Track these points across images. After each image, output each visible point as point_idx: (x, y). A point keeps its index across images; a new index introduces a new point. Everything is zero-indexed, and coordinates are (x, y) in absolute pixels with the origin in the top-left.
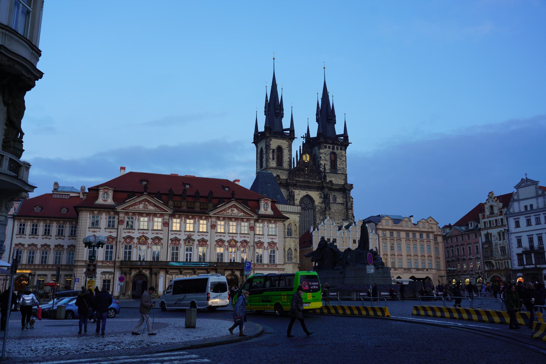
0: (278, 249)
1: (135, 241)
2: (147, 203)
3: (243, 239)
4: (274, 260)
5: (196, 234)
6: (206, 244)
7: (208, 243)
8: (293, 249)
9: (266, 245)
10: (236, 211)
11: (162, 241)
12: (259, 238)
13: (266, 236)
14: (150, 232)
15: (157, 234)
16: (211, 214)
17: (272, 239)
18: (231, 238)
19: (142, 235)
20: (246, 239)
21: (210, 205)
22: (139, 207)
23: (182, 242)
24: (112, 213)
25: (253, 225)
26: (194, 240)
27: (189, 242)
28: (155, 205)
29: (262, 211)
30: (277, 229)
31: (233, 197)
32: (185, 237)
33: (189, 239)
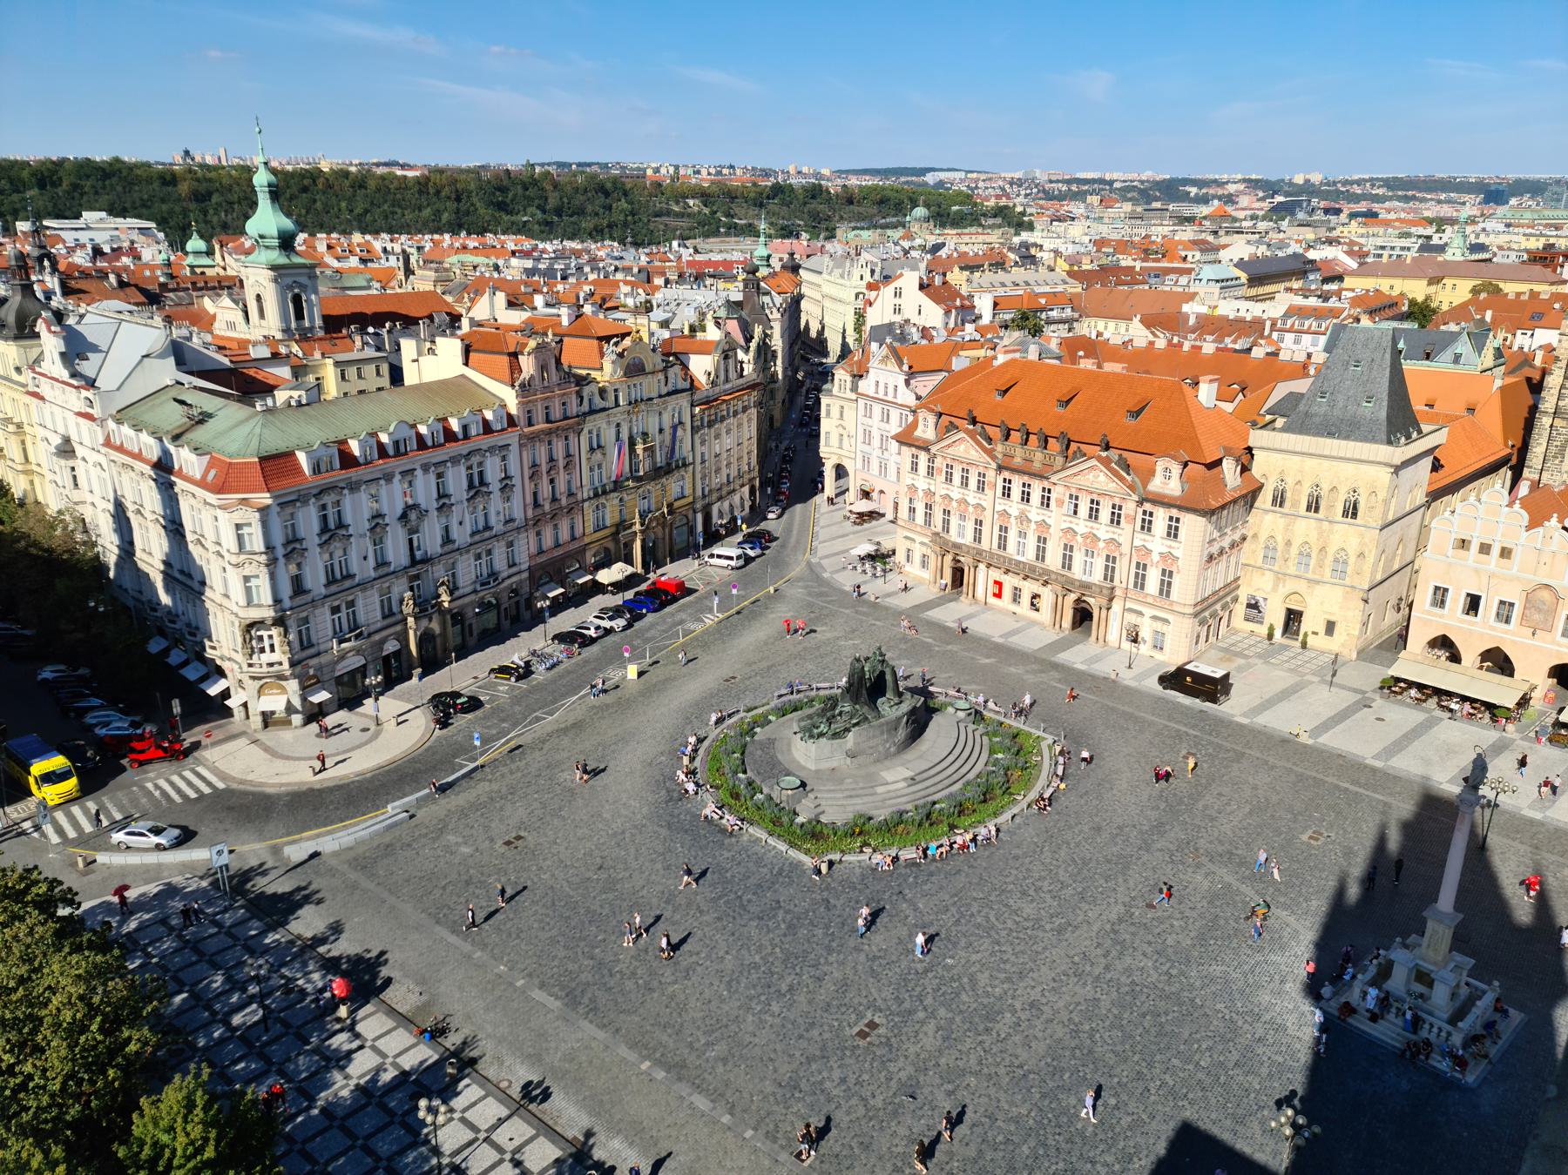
4: (1168, 593)
9: (1155, 557)
10: (1102, 478)
13: (1157, 540)
14: (972, 494)
16: (1054, 479)
23: (1012, 520)
29: (1157, 485)
33: (1023, 518)
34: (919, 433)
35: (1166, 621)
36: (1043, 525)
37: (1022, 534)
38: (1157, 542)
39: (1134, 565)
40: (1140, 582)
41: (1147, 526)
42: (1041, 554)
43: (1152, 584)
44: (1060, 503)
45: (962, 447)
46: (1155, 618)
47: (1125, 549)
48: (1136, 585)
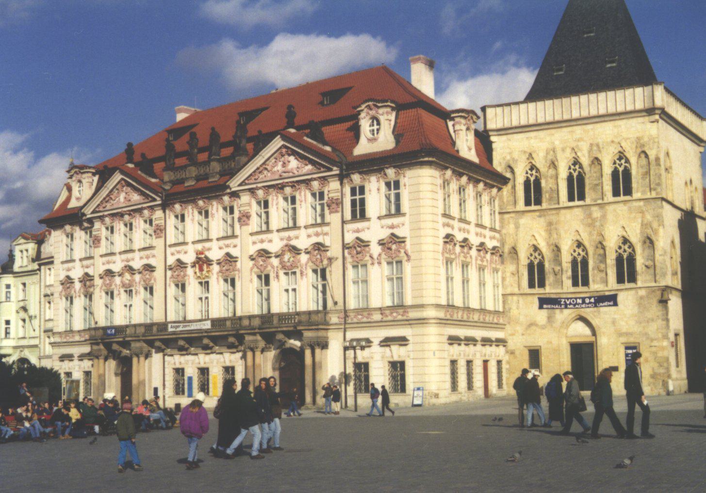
0: (409, 260)
2: (129, 189)
5: (214, 245)
7: (238, 264)
8: (635, 238)
10: (293, 163)
11: (155, 274)
12: (358, 231)
18: (285, 242)
20: (320, 239)
22: (119, 202)
23: (190, 271)
26: (208, 262)
27: (201, 270)
29: (363, 148)
31: (290, 125)
34: (73, 204)
35: (402, 341)
41: (359, 212)
45: (122, 196)
46: (387, 342)
47: (335, 250)
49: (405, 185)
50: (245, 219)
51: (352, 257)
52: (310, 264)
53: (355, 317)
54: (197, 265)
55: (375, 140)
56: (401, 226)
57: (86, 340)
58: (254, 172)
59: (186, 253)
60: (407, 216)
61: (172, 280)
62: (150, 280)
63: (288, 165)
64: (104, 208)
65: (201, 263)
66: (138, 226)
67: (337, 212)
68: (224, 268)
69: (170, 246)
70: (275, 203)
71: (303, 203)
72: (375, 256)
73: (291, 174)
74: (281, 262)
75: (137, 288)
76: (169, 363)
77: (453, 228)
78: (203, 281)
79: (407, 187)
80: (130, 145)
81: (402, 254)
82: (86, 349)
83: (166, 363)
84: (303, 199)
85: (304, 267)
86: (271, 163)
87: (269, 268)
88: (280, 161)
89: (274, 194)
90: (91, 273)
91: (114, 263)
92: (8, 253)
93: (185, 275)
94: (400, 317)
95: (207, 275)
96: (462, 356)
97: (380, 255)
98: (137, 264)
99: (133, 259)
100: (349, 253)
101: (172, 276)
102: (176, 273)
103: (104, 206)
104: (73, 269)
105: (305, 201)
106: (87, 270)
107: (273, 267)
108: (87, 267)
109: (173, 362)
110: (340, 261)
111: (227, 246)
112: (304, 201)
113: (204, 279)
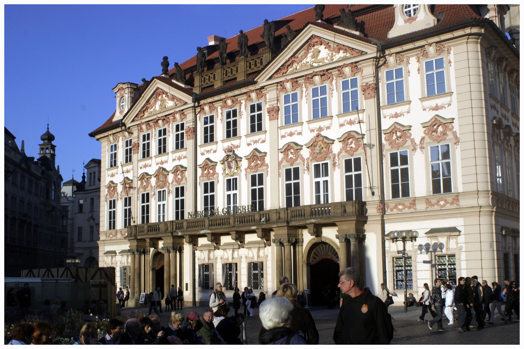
1: (153, 181)
2: (164, 96)
3: (348, 128)
6: (263, 164)
7: (267, 160)
9: (417, 133)
10: (324, 52)
11: (186, 173)
12: (396, 116)
13: (416, 105)
15: (179, 159)
17: (437, 108)
18: (316, 133)
19: (157, 168)
21: (267, 56)
23: (219, 168)
24: (126, 134)
25: (371, 80)
26: (237, 159)
27: (230, 167)
28: (173, 98)
30: (452, 69)
32: (223, 155)
34: (118, 117)
36: (257, 156)
37: (232, 184)
38: (415, 114)
39: (387, 161)
40: (401, 185)
41: (397, 95)
42: (258, 196)
43: (420, 183)
44: (274, 111)
45: (159, 103)
47: (371, 138)
48: (395, 194)
49: (450, 62)
50: (273, 113)
51: (390, 144)
52: (344, 153)
53: (396, 207)
54: (226, 163)
55: (414, 19)
56: (446, 106)
57: (125, 238)
58: (283, 66)
59: (215, 152)
60: (454, 96)
61: (202, 178)
62: (182, 180)
63: (317, 55)
64: (141, 117)
65: (230, 160)
66: (171, 130)
67: (371, 97)
68: (252, 164)
69: (201, 146)
70: (304, 94)
71: (335, 93)
72: (418, 141)
73: (321, 64)
74: (312, 154)
75: (170, 189)
76: (199, 259)
77: (498, 112)
78: (232, 178)
79: (452, 64)
80: (166, 58)
81: (450, 135)
82: (126, 246)
83: (196, 259)
84: (335, 87)
85: (336, 158)
86: (299, 56)
87: (299, 161)
88: (308, 52)
89: (304, 86)
90: (131, 178)
91: (150, 166)
92: (82, 175)
93: (214, 173)
94: (448, 206)
95: (236, 171)
96: (511, 250)
97: (423, 139)
98: (169, 167)
99: (166, 162)
100: (386, 139)
101: (202, 174)
102: (206, 172)
103: (142, 115)
104: (116, 175)
105: (336, 88)
106: (126, 175)
107: (303, 160)
108: (128, 172)
109: (202, 258)
110: (375, 151)
111: (256, 142)
112: (335, 90)
113: (232, 176)
